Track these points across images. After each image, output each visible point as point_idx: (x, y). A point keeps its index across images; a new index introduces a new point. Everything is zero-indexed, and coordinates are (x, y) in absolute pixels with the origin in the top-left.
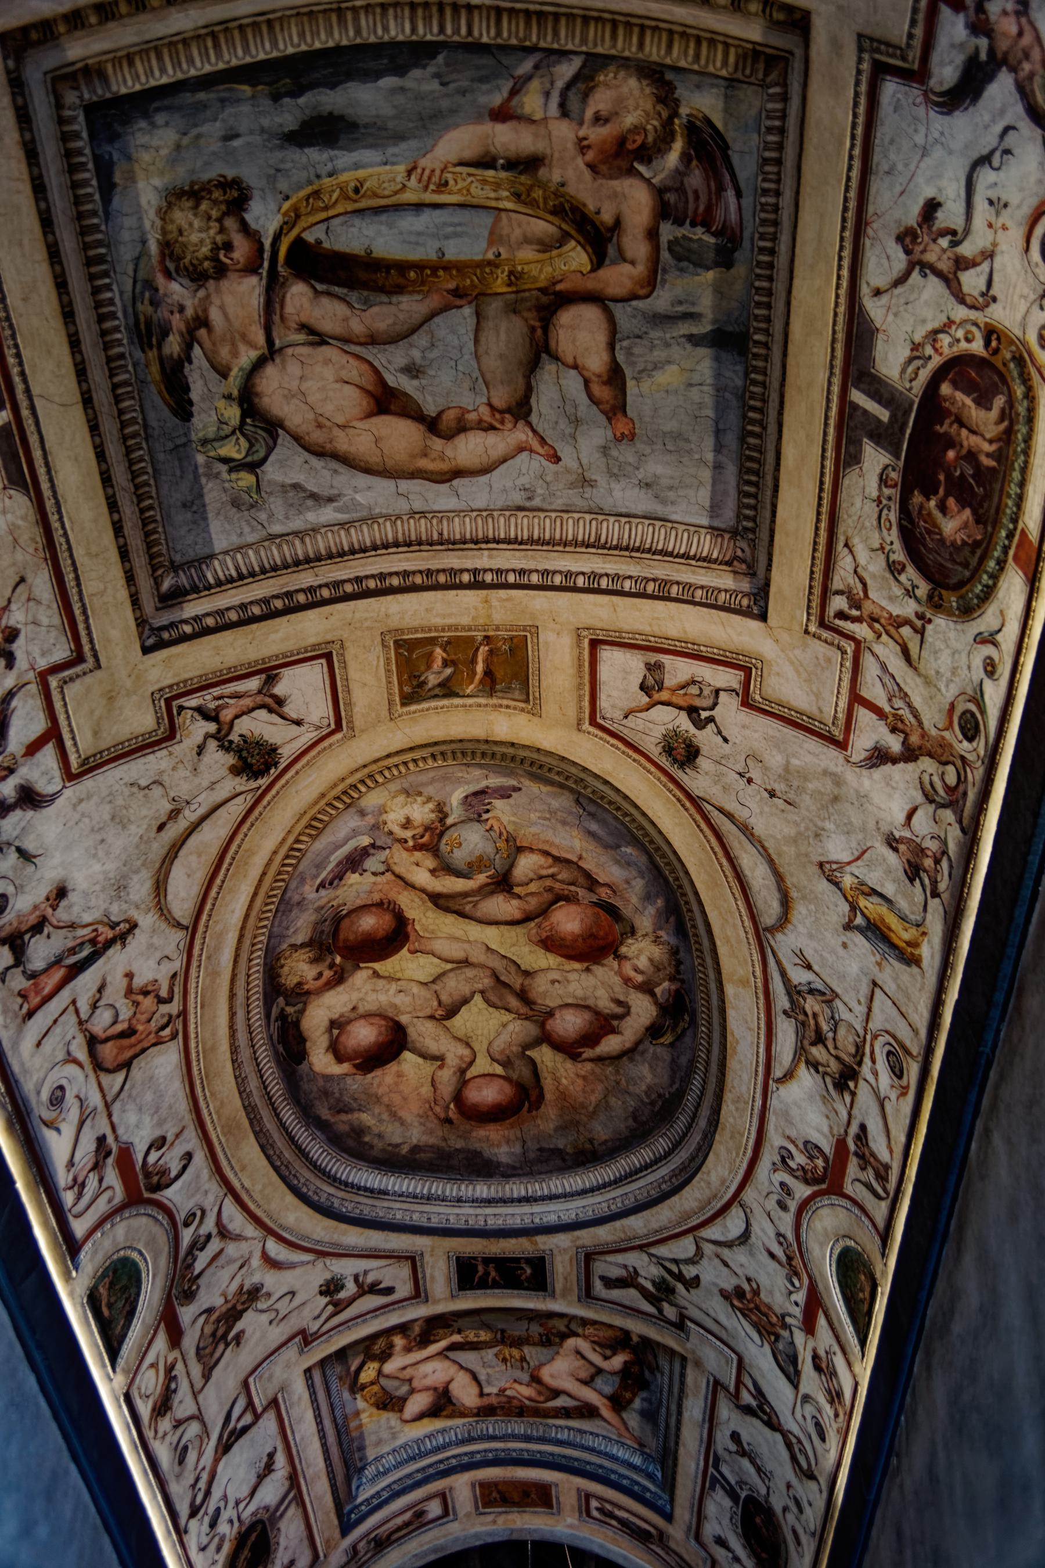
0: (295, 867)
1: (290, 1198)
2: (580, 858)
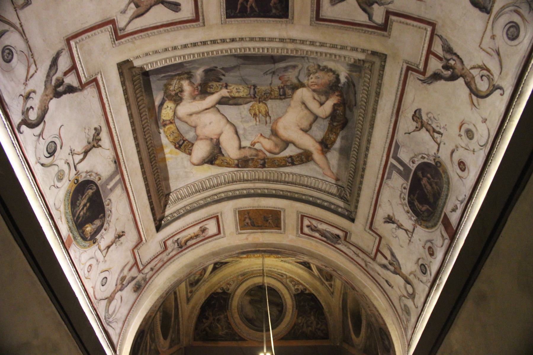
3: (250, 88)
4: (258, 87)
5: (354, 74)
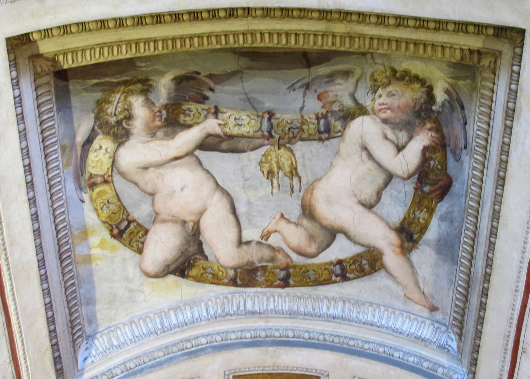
3: (263, 117)
4: (278, 115)
5: (461, 83)
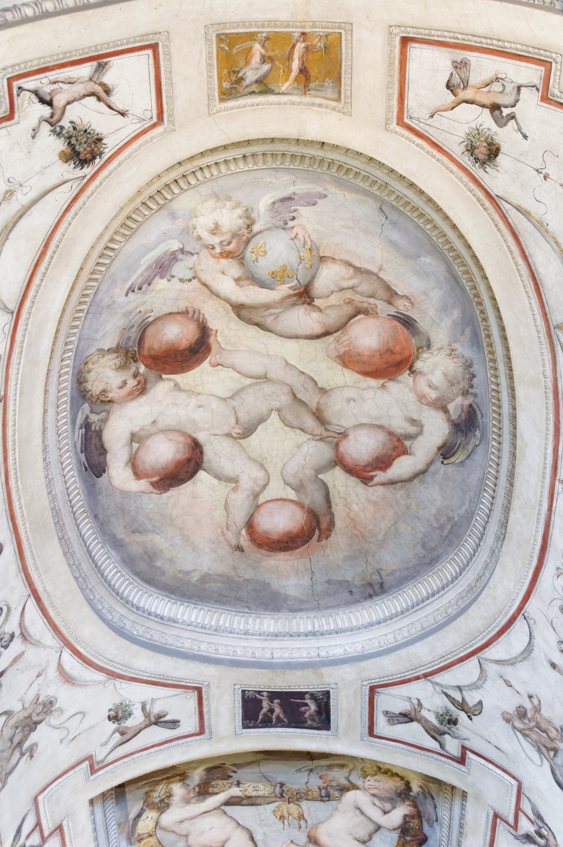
0: (108, 266)
1: (87, 610)
2: (381, 269)
3: (276, 786)
